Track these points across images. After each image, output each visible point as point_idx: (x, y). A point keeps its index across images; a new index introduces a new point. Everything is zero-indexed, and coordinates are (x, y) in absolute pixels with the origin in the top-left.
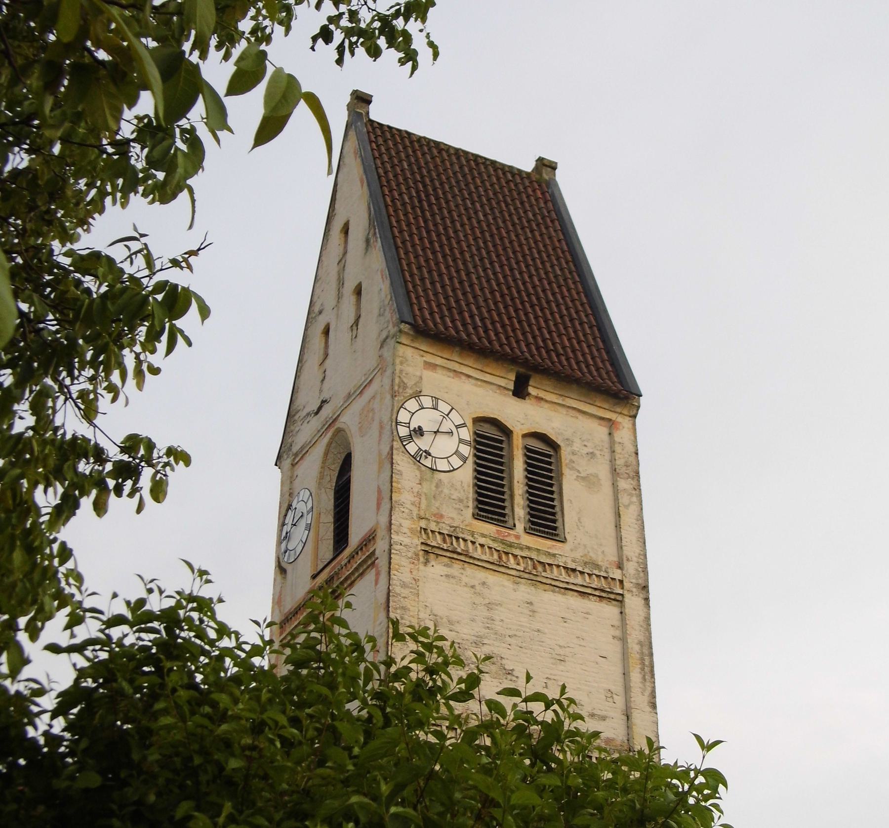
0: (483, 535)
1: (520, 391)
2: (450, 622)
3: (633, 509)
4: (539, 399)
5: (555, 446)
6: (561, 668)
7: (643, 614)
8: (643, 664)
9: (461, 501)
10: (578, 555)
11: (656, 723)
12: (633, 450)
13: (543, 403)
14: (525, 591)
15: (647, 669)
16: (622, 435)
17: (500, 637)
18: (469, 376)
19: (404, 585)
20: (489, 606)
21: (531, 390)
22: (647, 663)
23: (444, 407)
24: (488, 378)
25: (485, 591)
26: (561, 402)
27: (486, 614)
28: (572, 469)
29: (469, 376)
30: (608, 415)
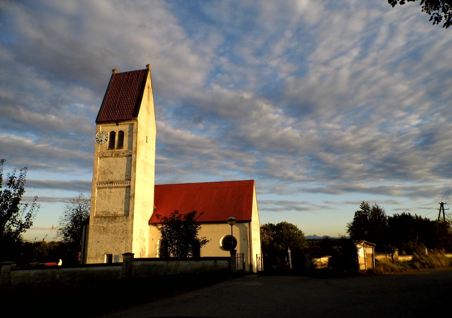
0: (109, 152)
1: (117, 125)
2: (103, 167)
3: (135, 139)
4: (120, 125)
5: (123, 132)
6: (121, 170)
7: (135, 157)
8: (134, 165)
9: (106, 147)
10: (125, 150)
11: (135, 175)
12: (137, 127)
13: (121, 125)
14: (116, 159)
15: (135, 166)
16: (135, 126)
17: (111, 168)
18: (108, 126)
19: (95, 164)
20: (110, 163)
21: (119, 124)
22: (135, 165)
23: (104, 133)
24: (111, 124)
25: (109, 161)
26: (124, 124)
27: (109, 164)
28: (126, 135)
29: (108, 126)
30: (133, 123)
